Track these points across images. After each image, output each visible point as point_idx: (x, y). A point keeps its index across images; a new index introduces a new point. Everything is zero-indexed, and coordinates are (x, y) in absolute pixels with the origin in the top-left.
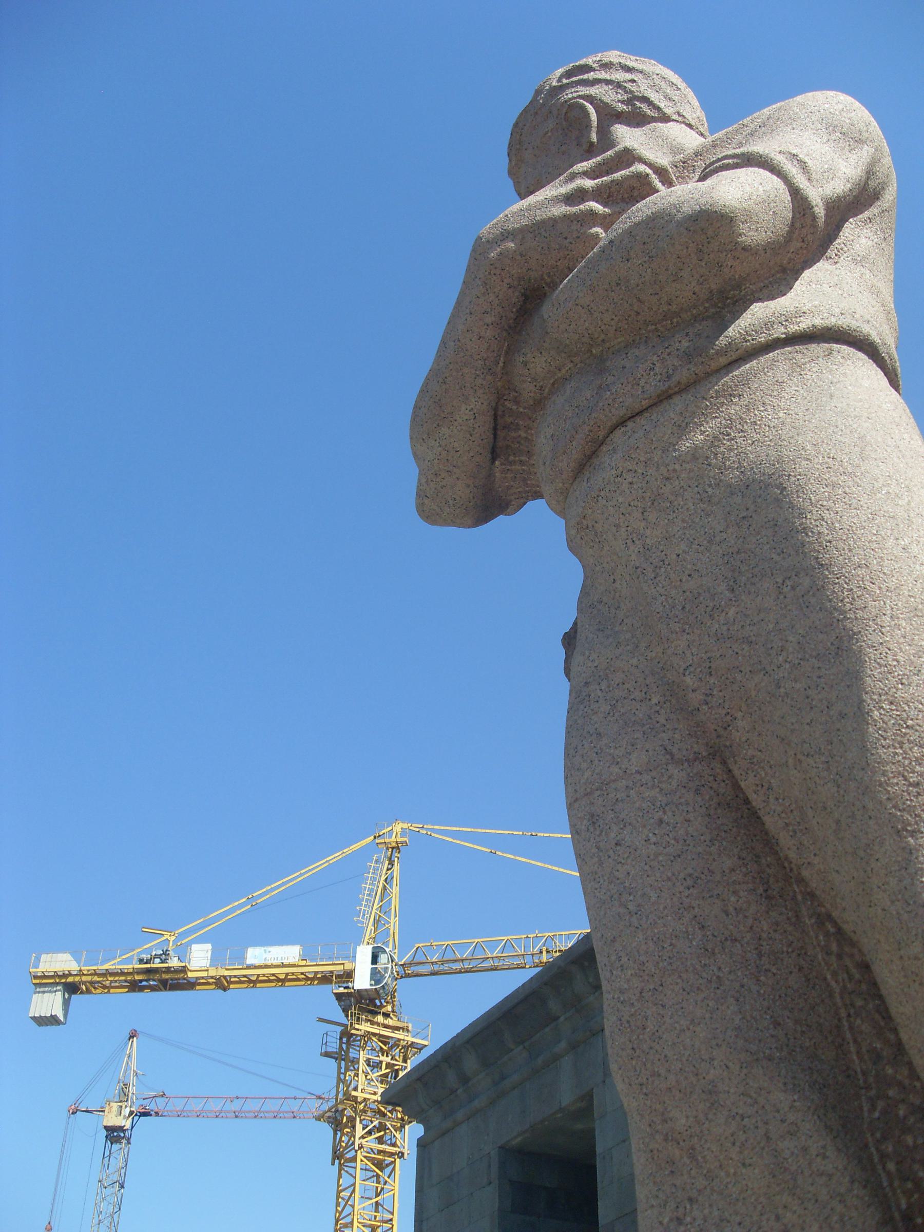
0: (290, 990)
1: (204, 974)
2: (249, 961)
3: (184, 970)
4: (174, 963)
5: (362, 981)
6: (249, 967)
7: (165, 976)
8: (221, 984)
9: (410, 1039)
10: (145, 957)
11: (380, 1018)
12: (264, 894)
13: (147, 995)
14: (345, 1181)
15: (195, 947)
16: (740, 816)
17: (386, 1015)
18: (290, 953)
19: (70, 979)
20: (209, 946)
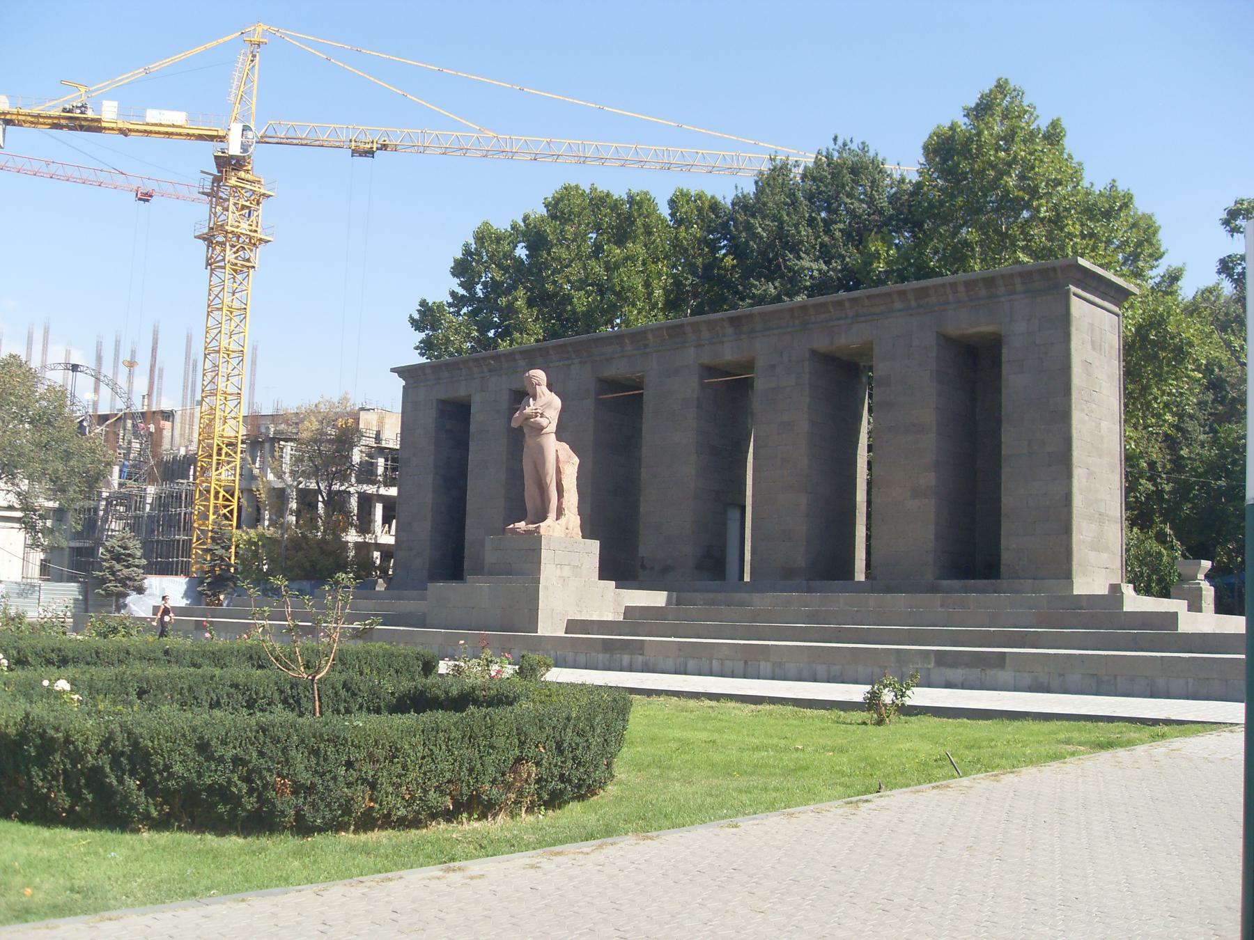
0: (174, 141)
1: (114, 125)
2: (149, 120)
3: (99, 120)
4: (90, 114)
5: (234, 149)
6: (147, 124)
7: (83, 123)
8: (124, 132)
9: (262, 191)
10: (68, 107)
11: (242, 174)
12: (154, 67)
13: (65, 133)
14: (215, 280)
15: (105, 103)
16: (536, 467)
17: (247, 171)
18: (177, 117)
19: (8, 117)
20: (116, 104)
